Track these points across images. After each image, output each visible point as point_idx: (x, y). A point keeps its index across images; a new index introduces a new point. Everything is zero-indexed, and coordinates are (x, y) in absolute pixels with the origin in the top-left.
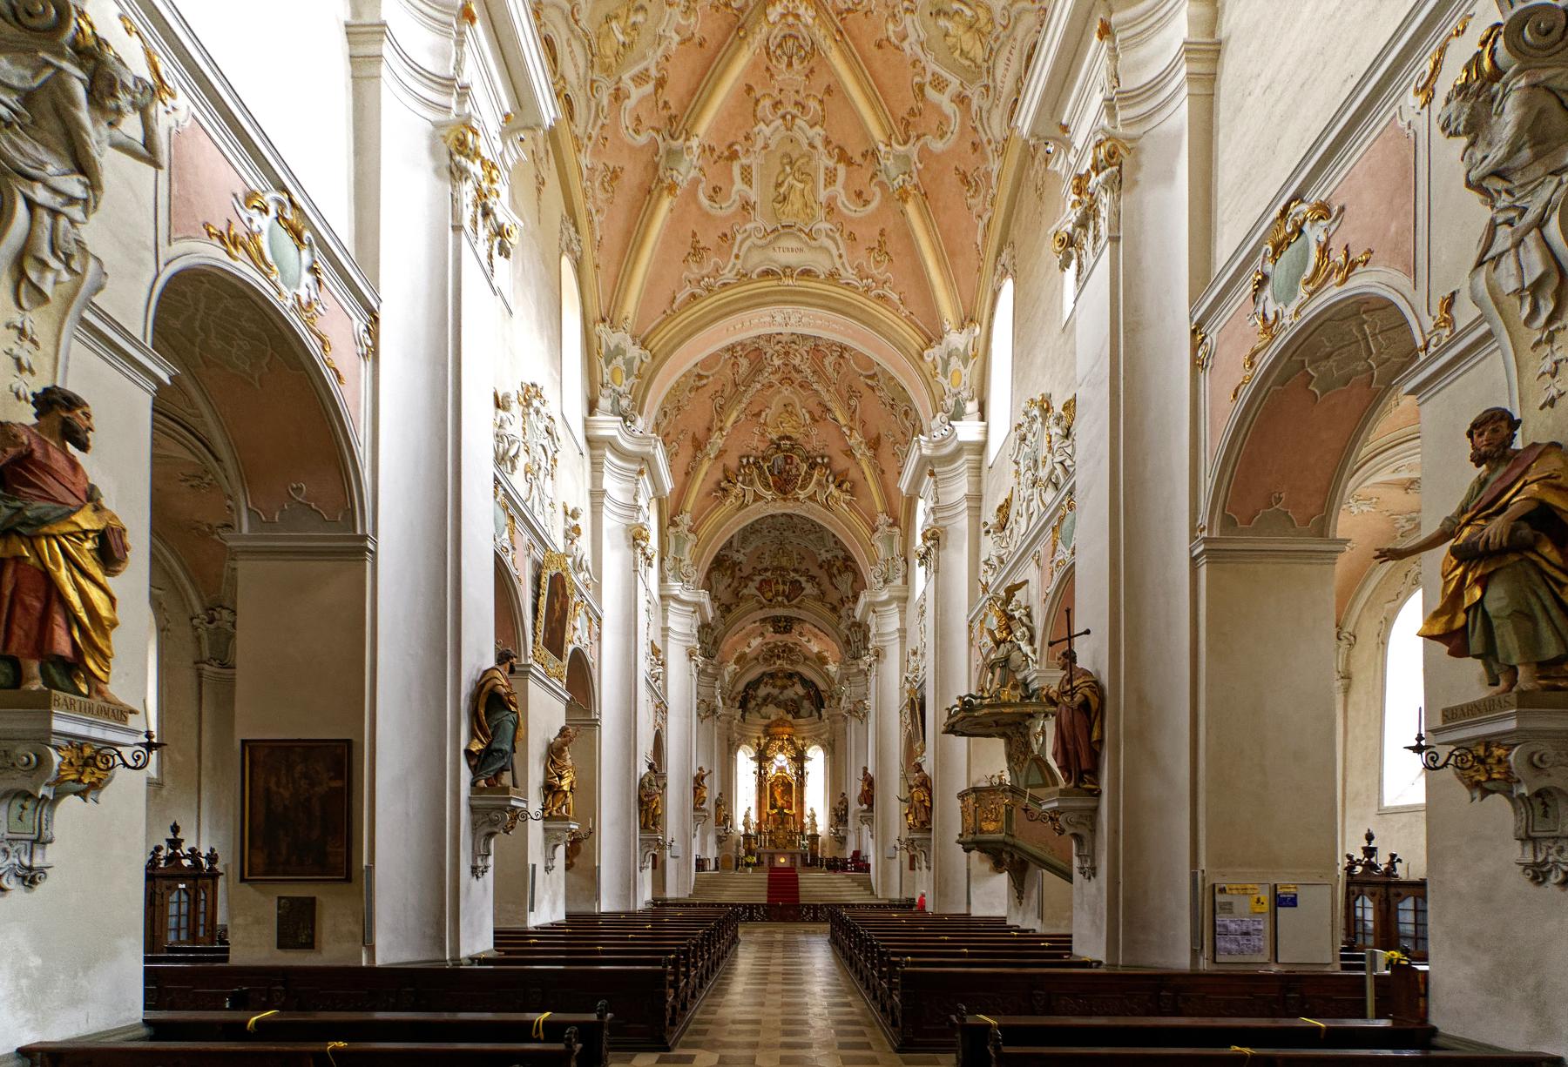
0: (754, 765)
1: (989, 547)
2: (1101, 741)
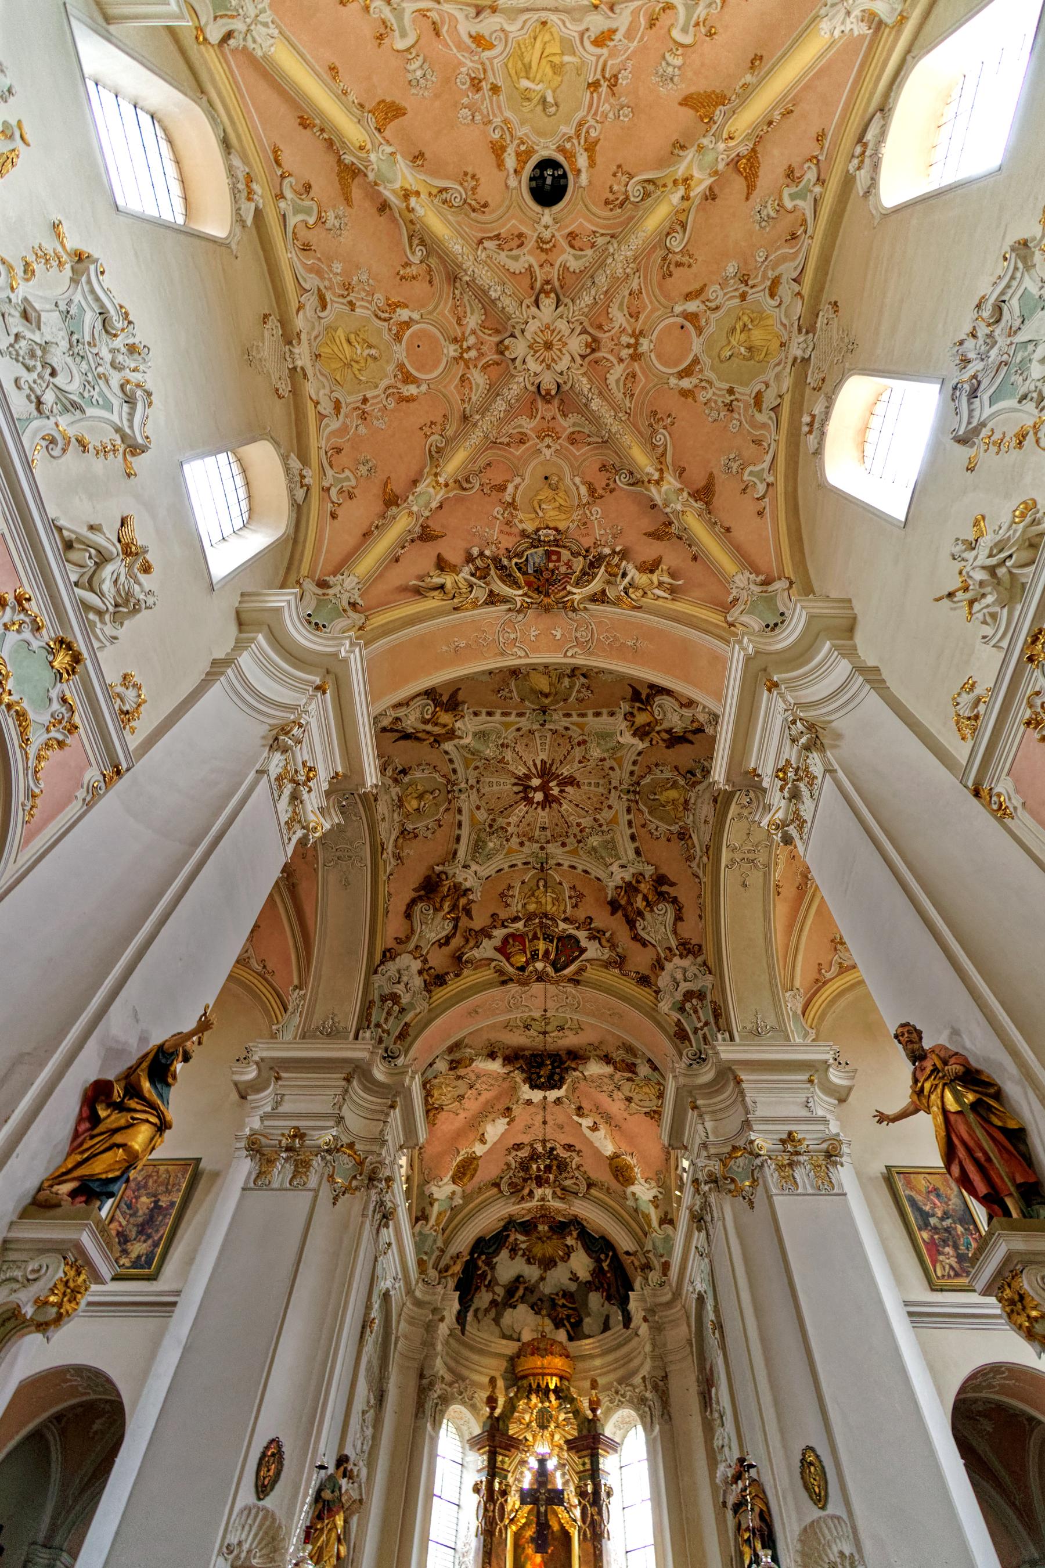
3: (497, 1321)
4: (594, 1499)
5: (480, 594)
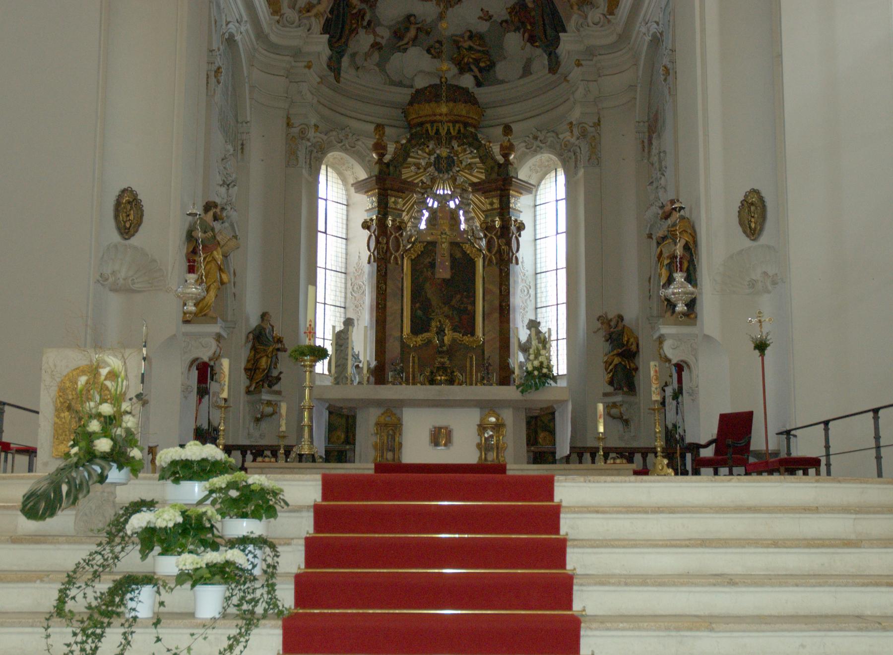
3: (381, 65)
4: (504, 235)
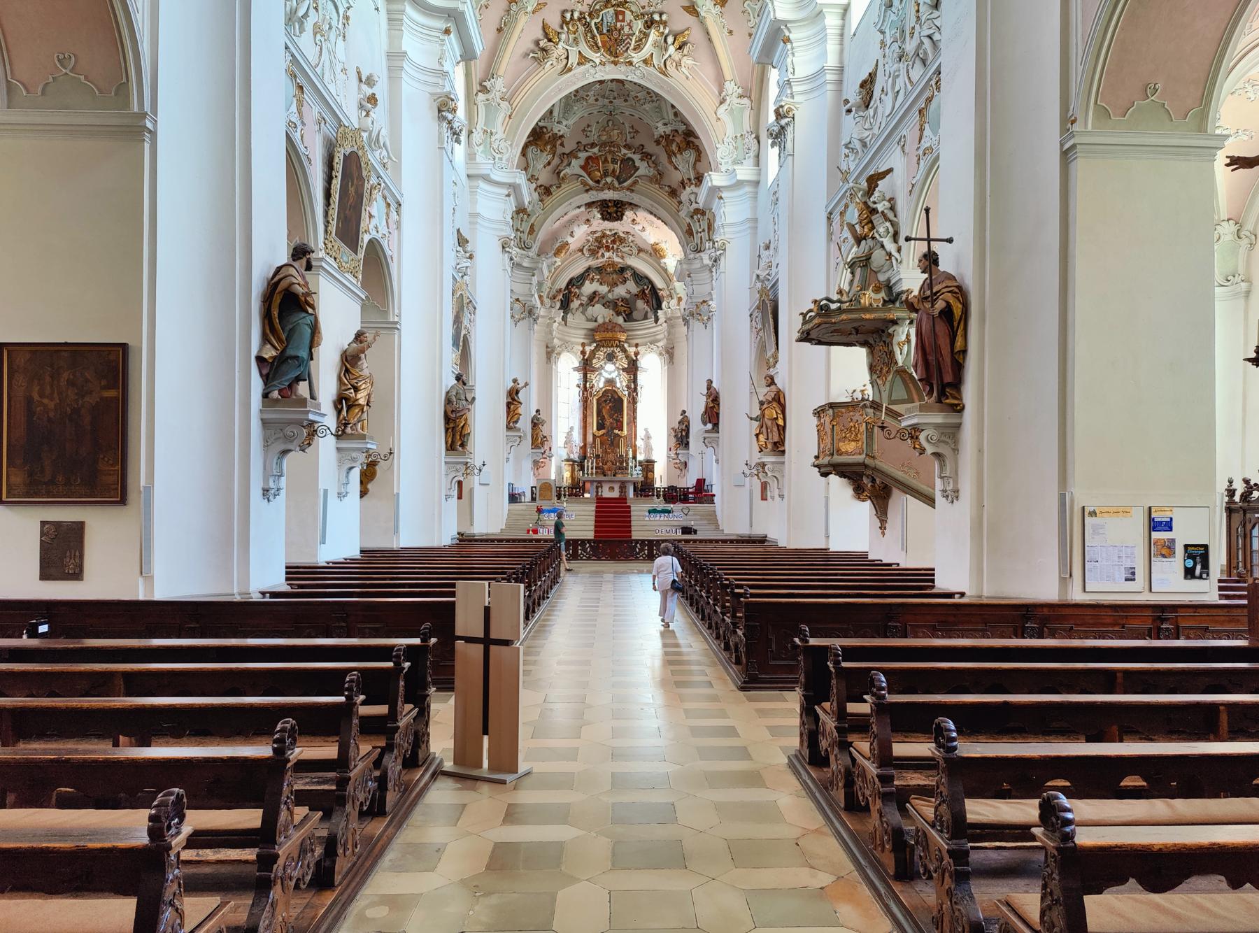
0: (577, 377)
1: (852, 128)
2: (964, 352)
3: (583, 313)
5: (574, 59)
